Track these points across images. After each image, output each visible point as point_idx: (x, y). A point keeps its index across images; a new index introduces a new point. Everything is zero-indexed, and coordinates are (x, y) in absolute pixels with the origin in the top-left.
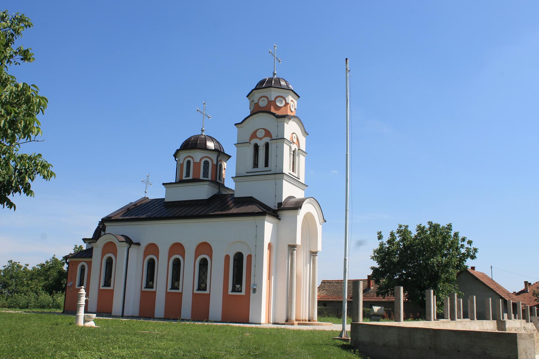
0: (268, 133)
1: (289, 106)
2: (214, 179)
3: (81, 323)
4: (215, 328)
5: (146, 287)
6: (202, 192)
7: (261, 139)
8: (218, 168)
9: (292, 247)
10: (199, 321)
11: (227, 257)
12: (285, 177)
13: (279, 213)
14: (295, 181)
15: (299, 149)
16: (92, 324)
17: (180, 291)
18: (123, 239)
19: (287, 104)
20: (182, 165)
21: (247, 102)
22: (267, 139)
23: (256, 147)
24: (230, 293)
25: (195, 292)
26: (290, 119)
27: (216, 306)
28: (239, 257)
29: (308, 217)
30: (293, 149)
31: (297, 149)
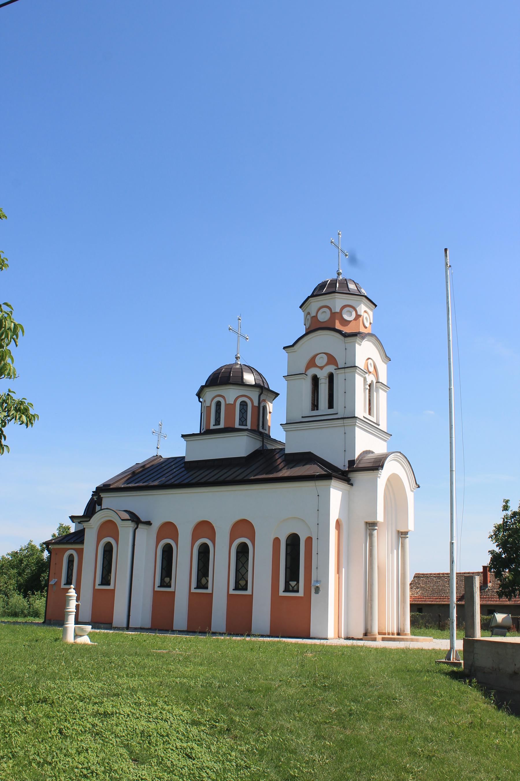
0: (331, 360)
1: (361, 319)
2: (256, 428)
3: (70, 638)
5: (161, 586)
6: (238, 446)
7: (321, 368)
8: (261, 412)
9: (371, 525)
10: (237, 635)
11: (277, 541)
13: (352, 475)
14: (373, 427)
15: (378, 382)
16: (85, 640)
17: (209, 591)
18: (127, 516)
19: (358, 316)
20: (209, 408)
21: (301, 315)
22: (331, 369)
23: (315, 380)
24: (281, 593)
25: (232, 592)
26: (363, 338)
27: (262, 613)
28: (293, 541)
29: (394, 479)
30: (369, 382)
31: (375, 382)
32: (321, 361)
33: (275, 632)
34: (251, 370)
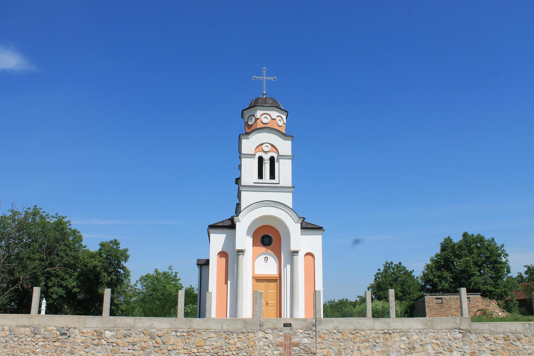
19: (257, 119)
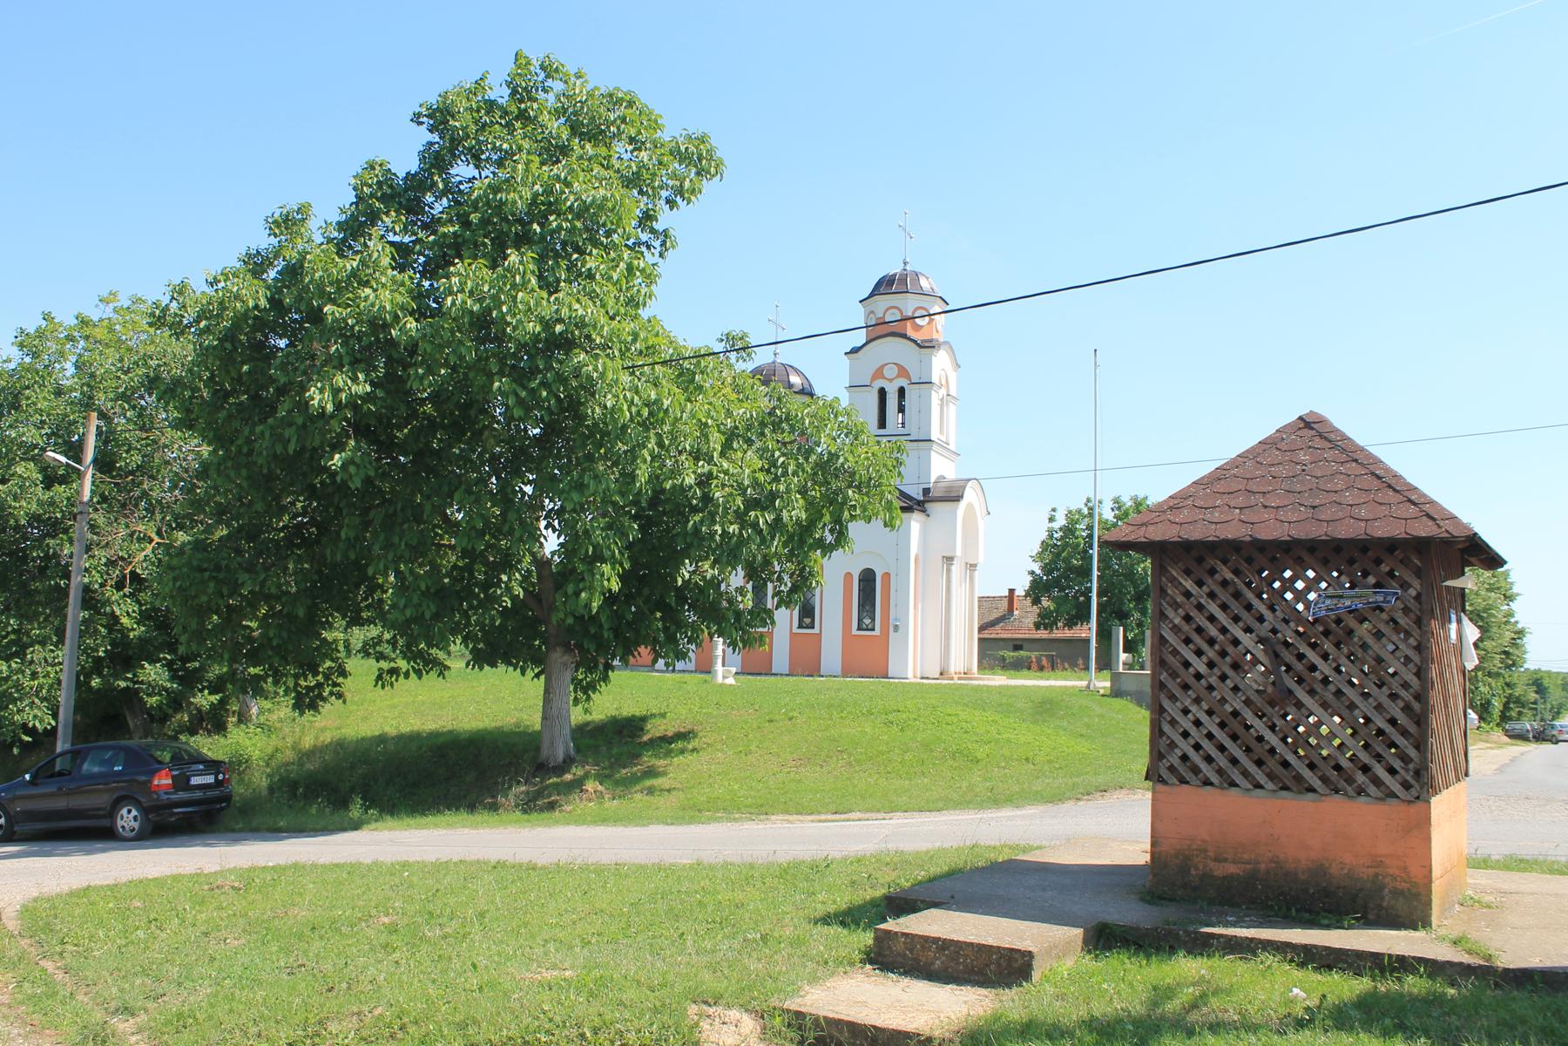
0: (903, 372)
3: (720, 679)
4: (830, 685)
9: (949, 560)
11: (848, 576)
12: (935, 447)
16: (731, 681)
22: (903, 382)
23: (882, 393)
25: (795, 630)
27: (832, 653)
28: (868, 578)
29: (970, 506)
32: (890, 372)
33: (846, 673)
34: (797, 371)
